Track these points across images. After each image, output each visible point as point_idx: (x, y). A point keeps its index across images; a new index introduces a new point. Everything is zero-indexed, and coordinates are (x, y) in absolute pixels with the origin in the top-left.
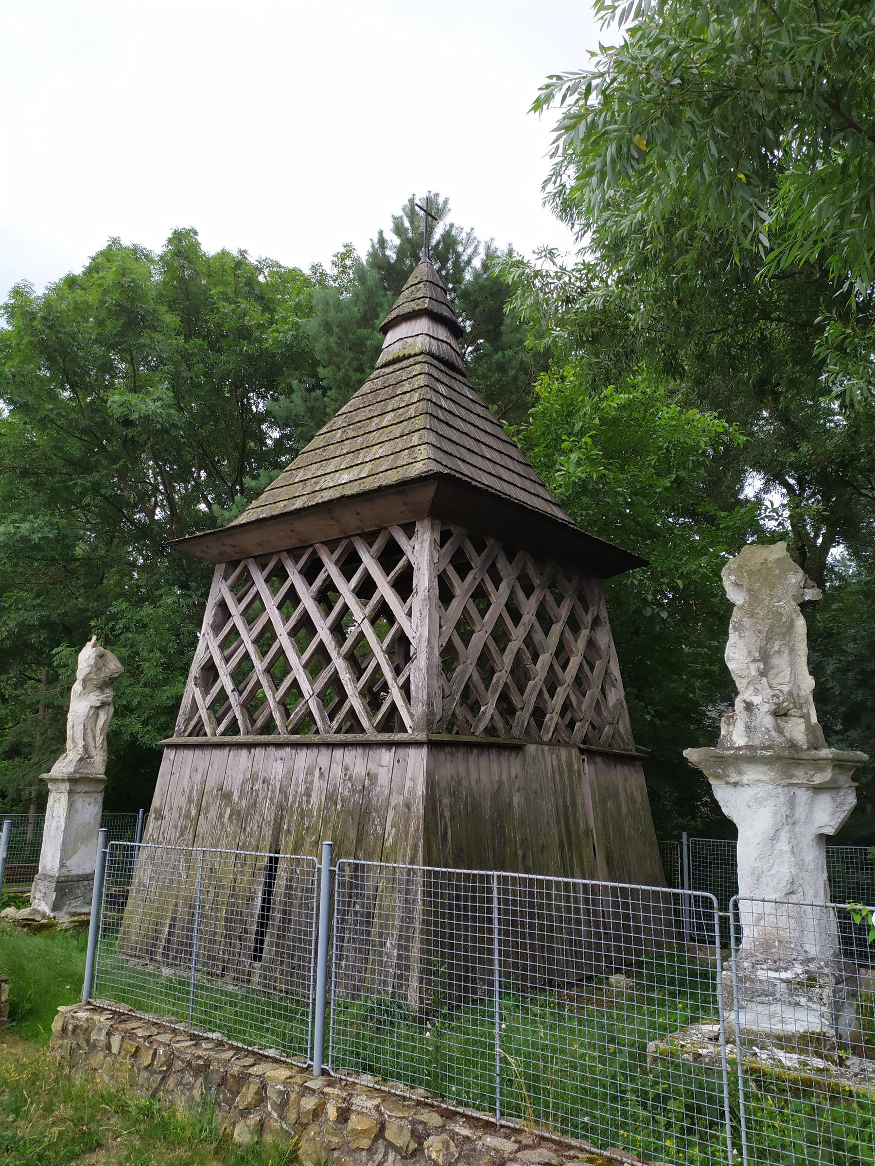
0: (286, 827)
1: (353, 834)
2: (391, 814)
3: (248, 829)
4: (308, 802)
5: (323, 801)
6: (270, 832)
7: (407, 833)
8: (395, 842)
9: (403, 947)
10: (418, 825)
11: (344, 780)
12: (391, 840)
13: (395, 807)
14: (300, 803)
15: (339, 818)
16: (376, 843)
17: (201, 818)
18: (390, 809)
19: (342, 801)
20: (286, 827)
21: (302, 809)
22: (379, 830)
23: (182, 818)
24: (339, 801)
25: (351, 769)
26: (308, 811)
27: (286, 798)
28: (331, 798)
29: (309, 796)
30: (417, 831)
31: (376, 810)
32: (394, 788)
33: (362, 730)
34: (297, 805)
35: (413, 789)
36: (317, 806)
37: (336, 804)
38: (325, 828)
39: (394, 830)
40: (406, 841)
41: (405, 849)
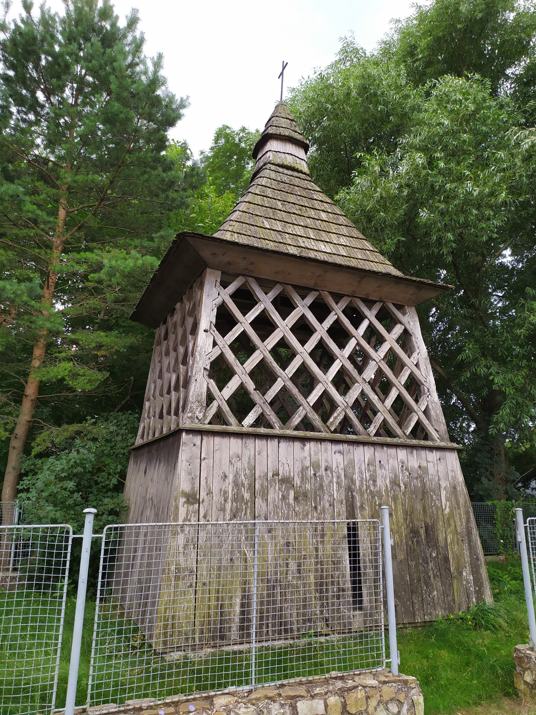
0: (358, 504)
1: (419, 507)
2: (443, 493)
3: (319, 508)
4: (375, 485)
5: (389, 485)
6: (344, 509)
7: (458, 505)
8: (451, 511)
9: (475, 571)
10: (466, 499)
11: (402, 471)
12: (448, 510)
13: (445, 488)
14: (368, 487)
15: (405, 496)
16: (437, 512)
17: (259, 501)
18: (442, 490)
19: (404, 484)
20: (358, 504)
21: (371, 491)
22: (437, 503)
23: (229, 501)
24: (402, 485)
25: (406, 462)
26: (377, 492)
27: (353, 481)
28: (395, 483)
29: (375, 481)
30: (466, 502)
31: (432, 490)
32: (441, 477)
33: (433, 440)
34: (365, 487)
35: (454, 478)
36: (384, 488)
37: (400, 487)
38: (395, 504)
39: (448, 503)
40: (459, 509)
41: (460, 515)
